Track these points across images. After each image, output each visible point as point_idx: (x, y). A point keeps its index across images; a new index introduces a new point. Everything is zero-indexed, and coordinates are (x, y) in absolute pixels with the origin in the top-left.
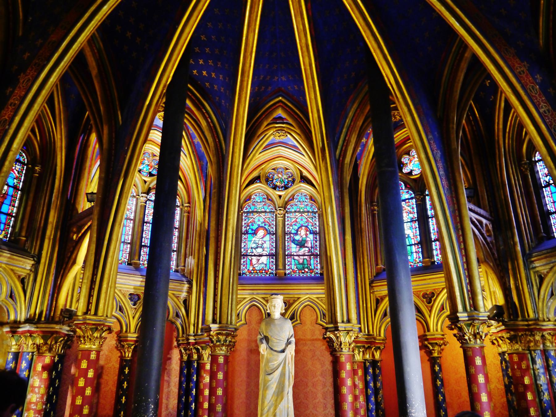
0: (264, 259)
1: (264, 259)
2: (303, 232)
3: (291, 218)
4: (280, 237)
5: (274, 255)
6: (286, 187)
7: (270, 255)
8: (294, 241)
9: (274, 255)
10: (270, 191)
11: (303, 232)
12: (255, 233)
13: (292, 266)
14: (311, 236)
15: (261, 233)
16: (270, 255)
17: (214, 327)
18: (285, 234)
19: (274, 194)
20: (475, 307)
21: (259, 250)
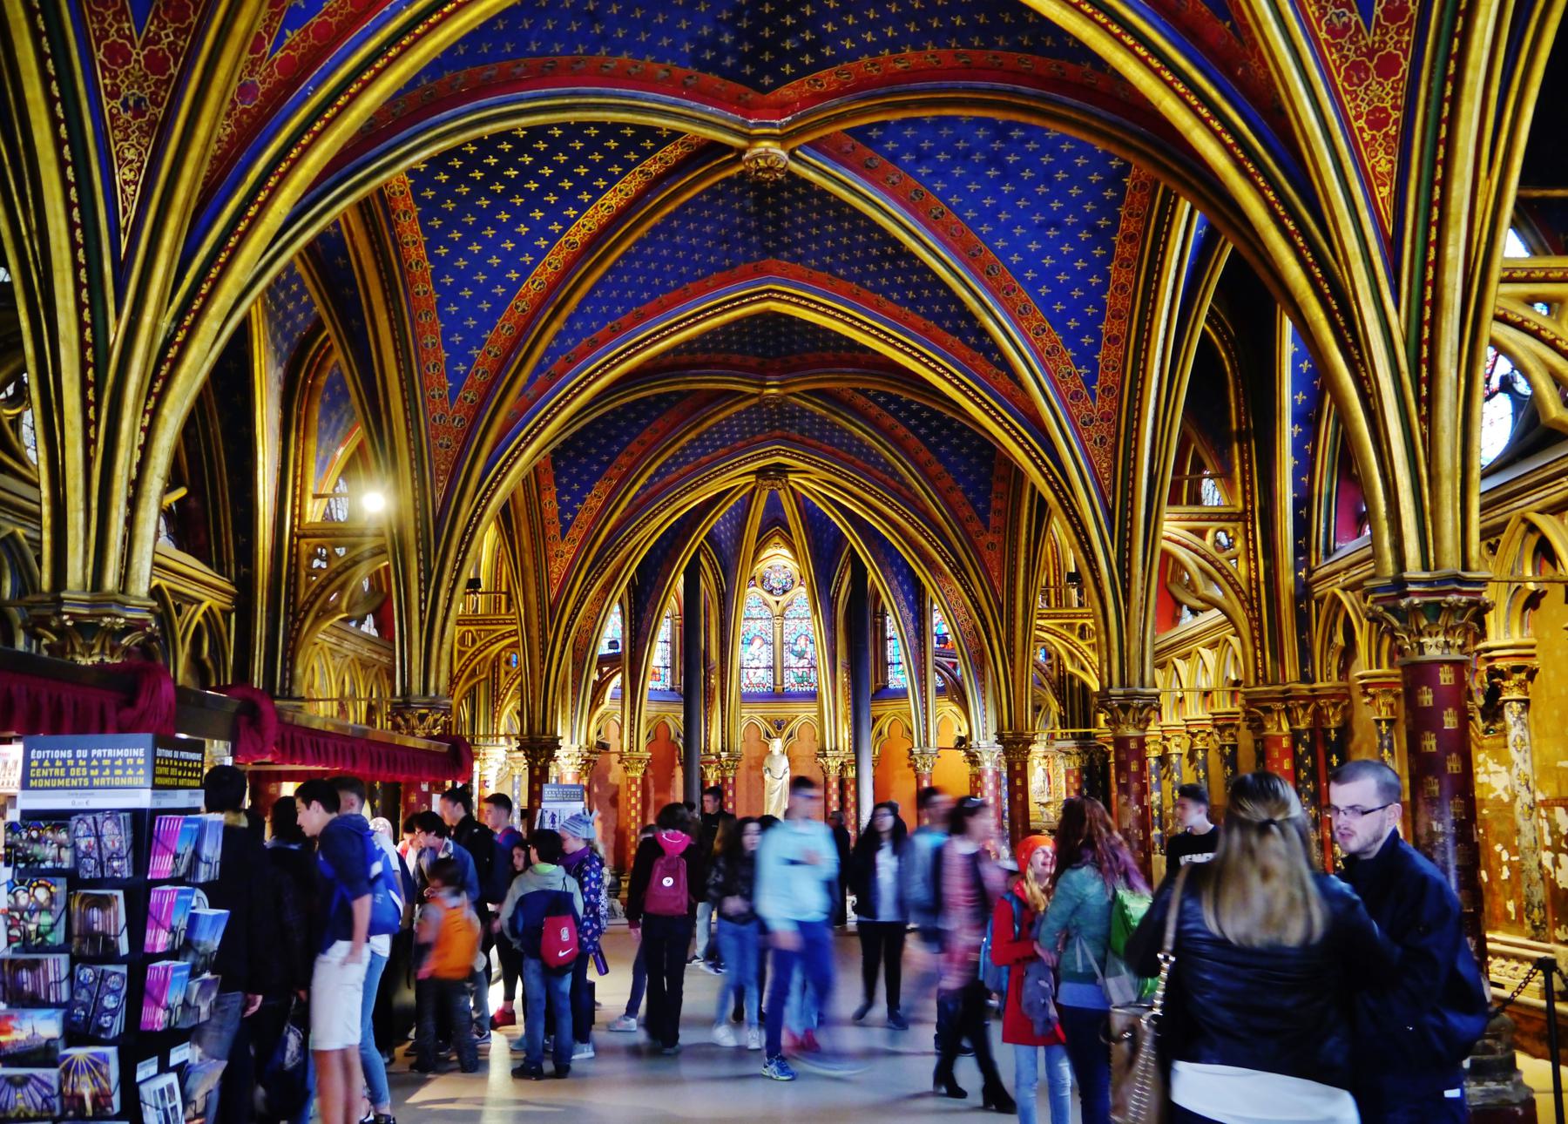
0: (761, 672)
1: (761, 672)
2: (802, 641)
3: (790, 625)
4: (779, 647)
5: (772, 668)
6: (785, 592)
7: (768, 668)
8: (792, 651)
9: (772, 668)
10: (767, 596)
11: (802, 641)
12: (751, 643)
13: (790, 681)
14: (810, 647)
15: (758, 642)
16: (768, 668)
17: (724, 754)
18: (783, 644)
19: (771, 599)
20: (927, 743)
21: (755, 663)
